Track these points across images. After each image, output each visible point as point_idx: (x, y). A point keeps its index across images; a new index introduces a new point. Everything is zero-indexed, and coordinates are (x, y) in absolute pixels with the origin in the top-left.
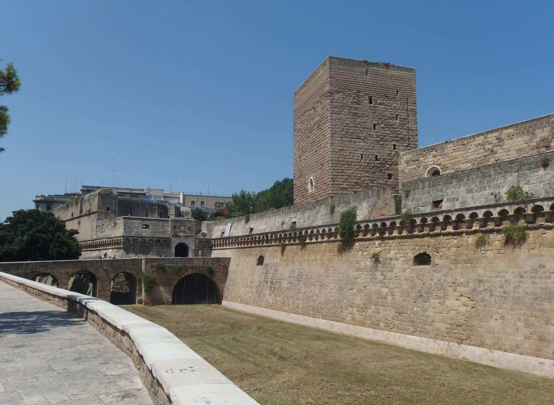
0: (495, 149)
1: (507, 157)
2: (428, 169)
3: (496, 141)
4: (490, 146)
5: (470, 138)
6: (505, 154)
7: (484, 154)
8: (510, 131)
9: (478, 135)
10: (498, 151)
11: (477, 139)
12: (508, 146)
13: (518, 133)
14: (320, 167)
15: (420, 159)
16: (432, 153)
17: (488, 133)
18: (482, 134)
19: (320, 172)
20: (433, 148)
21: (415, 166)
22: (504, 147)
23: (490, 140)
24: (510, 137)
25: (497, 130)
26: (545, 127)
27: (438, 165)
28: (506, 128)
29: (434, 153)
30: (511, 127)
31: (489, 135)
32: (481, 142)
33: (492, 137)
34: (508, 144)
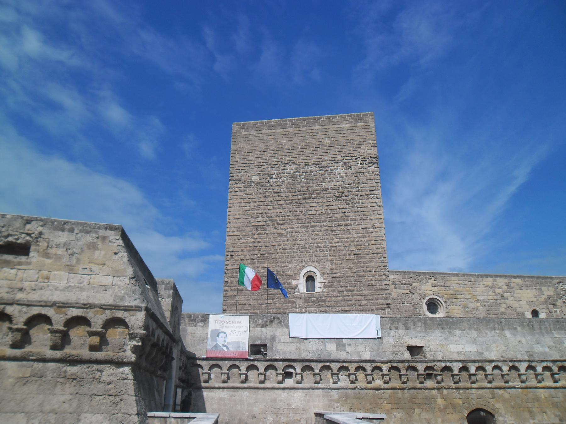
0: (506, 295)
1: (518, 306)
2: (427, 299)
3: (506, 287)
4: (500, 291)
5: (478, 276)
6: (516, 302)
7: (495, 297)
8: (518, 281)
9: (487, 276)
10: (509, 298)
11: (485, 279)
12: (519, 296)
13: (526, 285)
14: (348, 257)
15: (414, 284)
16: (430, 281)
17: (496, 276)
18: (491, 276)
19: (346, 265)
20: (433, 275)
21: (408, 291)
22: (515, 295)
23: (500, 284)
24: (520, 287)
25: (509, 276)
26: (549, 286)
27: (439, 296)
28: (515, 277)
29: (432, 281)
30: (519, 277)
31: (498, 280)
32: (490, 283)
33: (501, 282)
34: (518, 293)
